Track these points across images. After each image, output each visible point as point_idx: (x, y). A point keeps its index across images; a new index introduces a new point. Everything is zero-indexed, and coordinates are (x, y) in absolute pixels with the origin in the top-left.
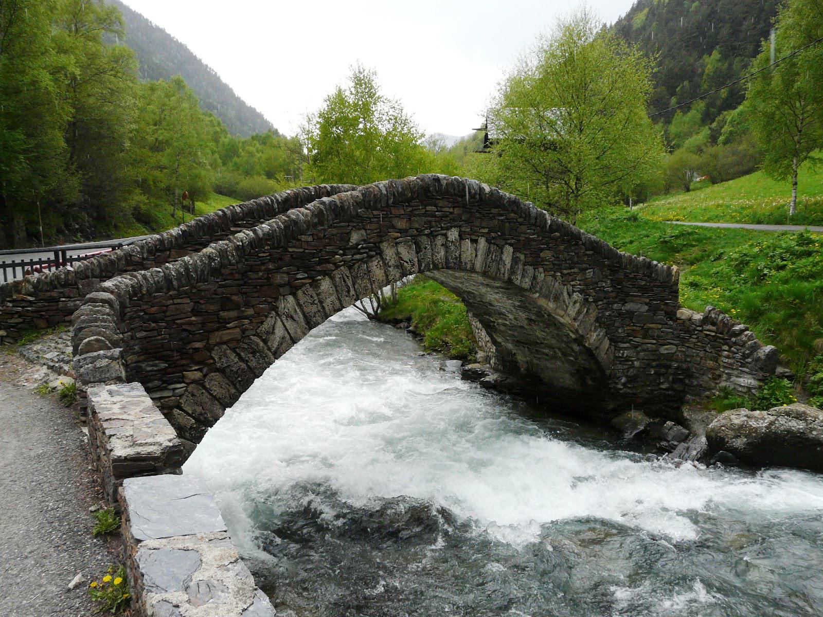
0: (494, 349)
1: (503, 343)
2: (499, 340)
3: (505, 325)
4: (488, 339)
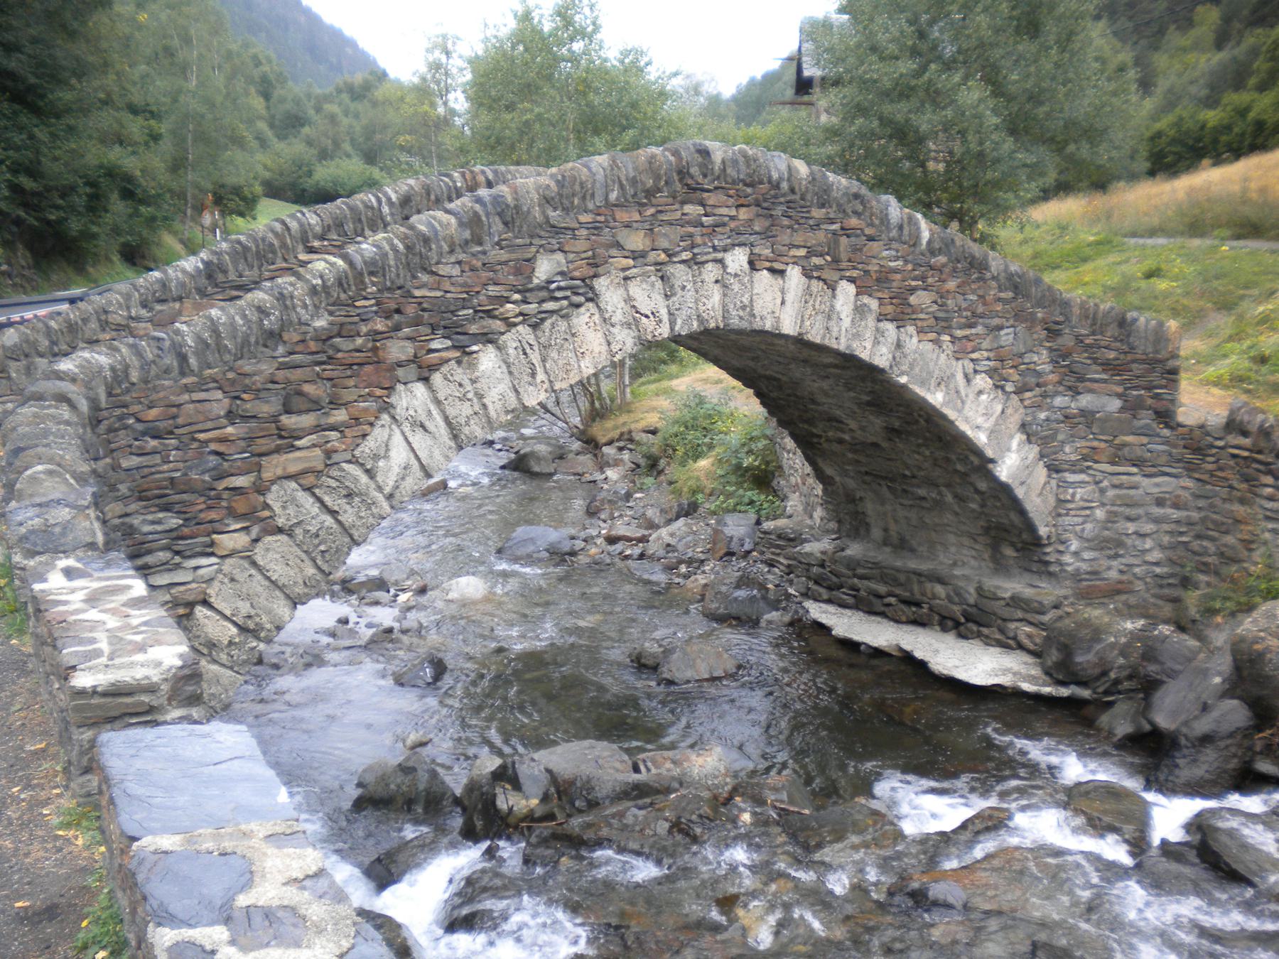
0: (819, 490)
1: (838, 479)
2: (829, 471)
3: (841, 441)
4: (808, 469)
